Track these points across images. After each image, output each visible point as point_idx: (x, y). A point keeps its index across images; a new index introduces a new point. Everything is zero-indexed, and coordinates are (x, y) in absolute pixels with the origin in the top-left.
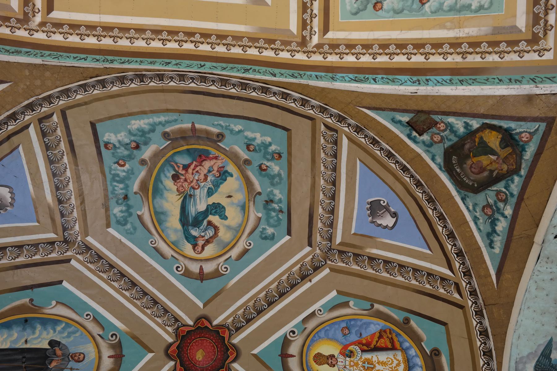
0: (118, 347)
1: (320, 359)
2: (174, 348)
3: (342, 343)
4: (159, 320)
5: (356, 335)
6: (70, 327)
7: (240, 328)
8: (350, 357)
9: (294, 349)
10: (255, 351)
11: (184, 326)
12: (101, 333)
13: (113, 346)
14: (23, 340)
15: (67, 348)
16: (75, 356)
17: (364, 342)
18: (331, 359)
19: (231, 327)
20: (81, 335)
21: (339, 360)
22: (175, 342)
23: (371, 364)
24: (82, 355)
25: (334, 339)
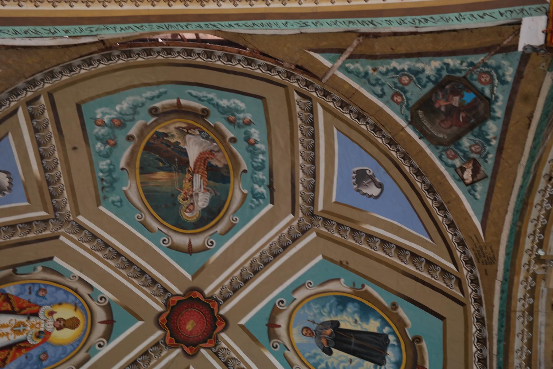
0: (272, 334)
1: (72, 324)
2: (219, 328)
3: (48, 343)
4: (234, 356)
5: (32, 356)
6: (313, 363)
7: (154, 346)
8: (40, 332)
9: (100, 329)
10: (140, 323)
11: (209, 348)
12: (287, 352)
13: (277, 337)
14: (353, 363)
15: (317, 344)
16: (310, 334)
17: (23, 351)
18: (60, 325)
19: (164, 346)
20: (304, 354)
21: (52, 326)
22: (219, 333)
23: (16, 330)
24: (304, 332)
25: (55, 346)
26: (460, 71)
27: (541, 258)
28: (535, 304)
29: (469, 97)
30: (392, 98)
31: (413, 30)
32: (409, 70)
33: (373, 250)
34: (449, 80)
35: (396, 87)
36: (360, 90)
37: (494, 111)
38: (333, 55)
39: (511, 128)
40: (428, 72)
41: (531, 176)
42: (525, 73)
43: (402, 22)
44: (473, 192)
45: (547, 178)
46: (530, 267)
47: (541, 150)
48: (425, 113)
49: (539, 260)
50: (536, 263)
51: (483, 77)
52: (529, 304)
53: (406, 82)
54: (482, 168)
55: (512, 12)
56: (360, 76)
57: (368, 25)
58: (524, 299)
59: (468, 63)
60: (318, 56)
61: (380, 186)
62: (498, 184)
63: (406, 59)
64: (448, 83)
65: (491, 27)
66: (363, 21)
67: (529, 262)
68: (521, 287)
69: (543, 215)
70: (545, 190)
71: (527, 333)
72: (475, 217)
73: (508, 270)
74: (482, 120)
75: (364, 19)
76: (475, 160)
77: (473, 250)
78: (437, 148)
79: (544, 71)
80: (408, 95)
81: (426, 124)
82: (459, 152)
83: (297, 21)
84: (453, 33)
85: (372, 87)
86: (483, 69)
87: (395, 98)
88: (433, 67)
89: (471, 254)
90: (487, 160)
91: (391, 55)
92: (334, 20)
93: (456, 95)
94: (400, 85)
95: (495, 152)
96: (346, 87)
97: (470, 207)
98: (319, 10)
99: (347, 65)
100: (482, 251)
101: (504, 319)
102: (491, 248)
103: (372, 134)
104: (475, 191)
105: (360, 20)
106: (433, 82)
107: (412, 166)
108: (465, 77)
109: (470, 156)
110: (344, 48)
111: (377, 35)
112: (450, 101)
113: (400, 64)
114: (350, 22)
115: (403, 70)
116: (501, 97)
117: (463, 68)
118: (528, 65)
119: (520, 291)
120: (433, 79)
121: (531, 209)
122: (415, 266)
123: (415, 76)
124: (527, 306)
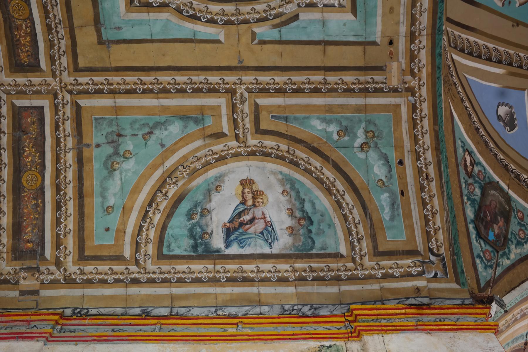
27: (410, 93)
28: (409, 43)
33: (496, 47)
35: (524, 225)
41: (443, 180)
45: (430, 178)
46: (419, 83)
48: (505, 209)
49: (411, 91)
50: (414, 88)
52: (415, 44)
58: (419, 48)
61: (499, 117)
67: (420, 89)
68: (424, 61)
69: (420, 140)
70: (426, 165)
71: (416, 14)
80: (516, 222)
81: (502, 199)
94: (523, 228)
101: (438, 26)
119: (424, 56)
120: (510, 243)
122: (469, 42)
124: (417, 41)
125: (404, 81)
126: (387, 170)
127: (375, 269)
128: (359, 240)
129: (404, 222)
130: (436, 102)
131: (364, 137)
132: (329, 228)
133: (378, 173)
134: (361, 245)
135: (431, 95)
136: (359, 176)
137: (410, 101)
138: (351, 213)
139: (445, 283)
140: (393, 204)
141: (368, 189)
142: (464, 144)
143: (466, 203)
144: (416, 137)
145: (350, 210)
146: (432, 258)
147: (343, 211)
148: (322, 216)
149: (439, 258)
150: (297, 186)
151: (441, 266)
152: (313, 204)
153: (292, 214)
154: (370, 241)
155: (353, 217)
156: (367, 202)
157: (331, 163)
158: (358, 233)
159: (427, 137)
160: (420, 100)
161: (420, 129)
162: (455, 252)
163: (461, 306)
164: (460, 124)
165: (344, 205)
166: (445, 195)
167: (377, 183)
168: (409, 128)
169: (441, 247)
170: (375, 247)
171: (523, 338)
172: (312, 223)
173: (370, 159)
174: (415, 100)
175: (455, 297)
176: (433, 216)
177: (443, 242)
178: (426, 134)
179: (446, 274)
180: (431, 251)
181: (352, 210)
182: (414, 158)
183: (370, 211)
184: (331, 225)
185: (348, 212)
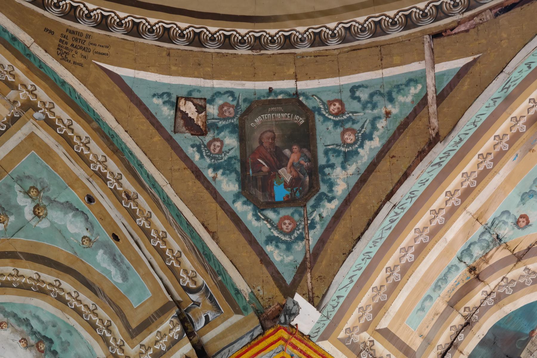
26: (315, 207)
27: (31, 110)
29: (280, 192)
30: (341, 102)
31: (395, 199)
32: (357, 153)
34: (313, 187)
35: (350, 119)
36: (380, 71)
37: (244, 203)
38: (445, 84)
39: (215, 206)
40: (338, 170)
41: (147, 185)
42: (264, 268)
43: (412, 196)
44: (166, 98)
45: (131, 195)
46: (28, 91)
47: (171, 218)
48: (296, 124)
49: (29, 106)
50: (28, 99)
51: (290, 224)
53: (346, 136)
54: (188, 135)
55: (334, 307)
56: (395, 90)
57: (441, 158)
59: (317, 223)
60: (459, 63)
62: (157, 138)
63: (370, 161)
64: (309, 184)
65: (335, 276)
66: (449, 155)
67: (36, 96)
69: (88, 156)
70: (117, 181)
72: (132, 76)
73: (40, 67)
74: (244, 183)
75: (449, 158)
76: (203, 133)
77: (88, 36)
78: (245, 100)
79: (254, 288)
80: (330, 125)
81: (283, 115)
82: (224, 123)
83: (518, 82)
84: (359, 234)
85: (372, 91)
86: (298, 232)
87: (337, 105)
88: (339, 181)
89: (82, 27)
90: (195, 149)
91: (389, 149)
92: (479, 124)
93: (291, 180)
94: (348, 125)
95: (199, 166)
96: (396, 59)
97: (148, 79)
98: (504, 114)
99: (420, 87)
100: (81, 48)
102: (81, 65)
103: (315, 27)
104: (164, 103)
105: (453, 154)
106: (324, 167)
107: (242, 42)
108: (305, 206)
109: (212, 131)
110: (440, 106)
111: (422, 155)
112: (290, 168)
113: (371, 149)
114: (461, 140)
115: (362, 146)
116: (255, 223)
117: (315, 213)
118: (271, 279)
120: (327, 170)
121: (104, 151)
123: (344, 152)
125: (12, 101)
126: (83, 219)
127: (142, 353)
128: (108, 328)
129: (139, 272)
130: (65, 94)
131: (30, 200)
132: (71, 335)
133: (76, 231)
134: (114, 333)
135: (52, 93)
136: (59, 251)
137: (39, 119)
138: (80, 302)
139: (222, 322)
140: (114, 259)
141: (78, 259)
142: (169, 94)
143: (214, 178)
144: (80, 155)
145: (76, 299)
146: (194, 297)
147: (71, 305)
148: (54, 326)
149: (201, 292)
150: (8, 309)
151: (208, 302)
152: (38, 318)
153: (27, 344)
154: (119, 321)
155: (85, 305)
156: (87, 276)
157: (21, 257)
158: (101, 320)
159: (93, 145)
160: (47, 109)
161: (78, 142)
162: (216, 270)
163: (254, 341)
164: (142, 75)
165: (67, 298)
166: (161, 203)
167: (83, 244)
168: (66, 151)
169: (196, 276)
170: (127, 326)
171: (458, 269)
172: (51, 341)
173: (56, 222)
174: (42, 113)
175: (243, 334)
176: (165, 243)
177: (194, 269)
178: (89, 142)
179: (218, 310)
180: (187, 289)
181: (78, 298)
182: (100, 181)
183: (97, 285)
184: (71, 330)
185: (76, 302)
